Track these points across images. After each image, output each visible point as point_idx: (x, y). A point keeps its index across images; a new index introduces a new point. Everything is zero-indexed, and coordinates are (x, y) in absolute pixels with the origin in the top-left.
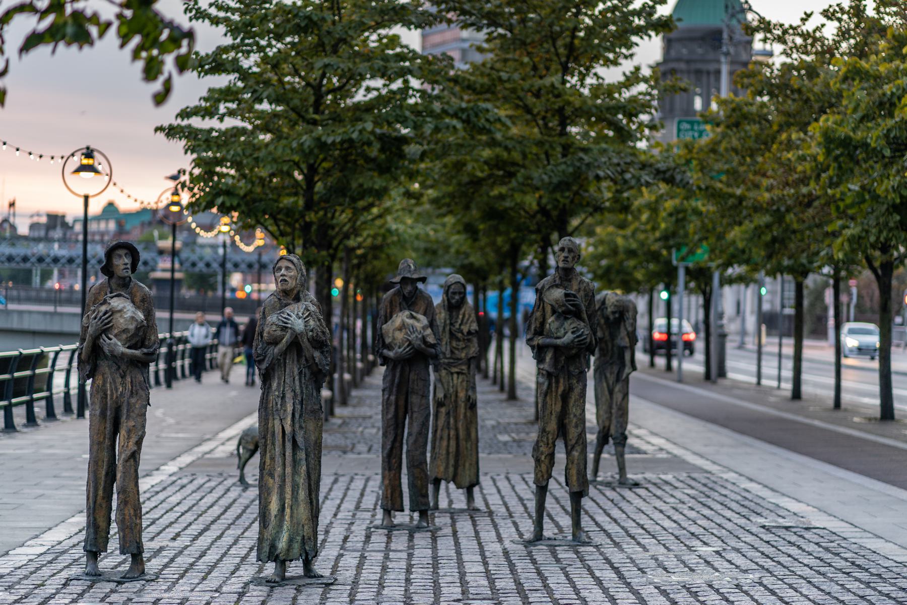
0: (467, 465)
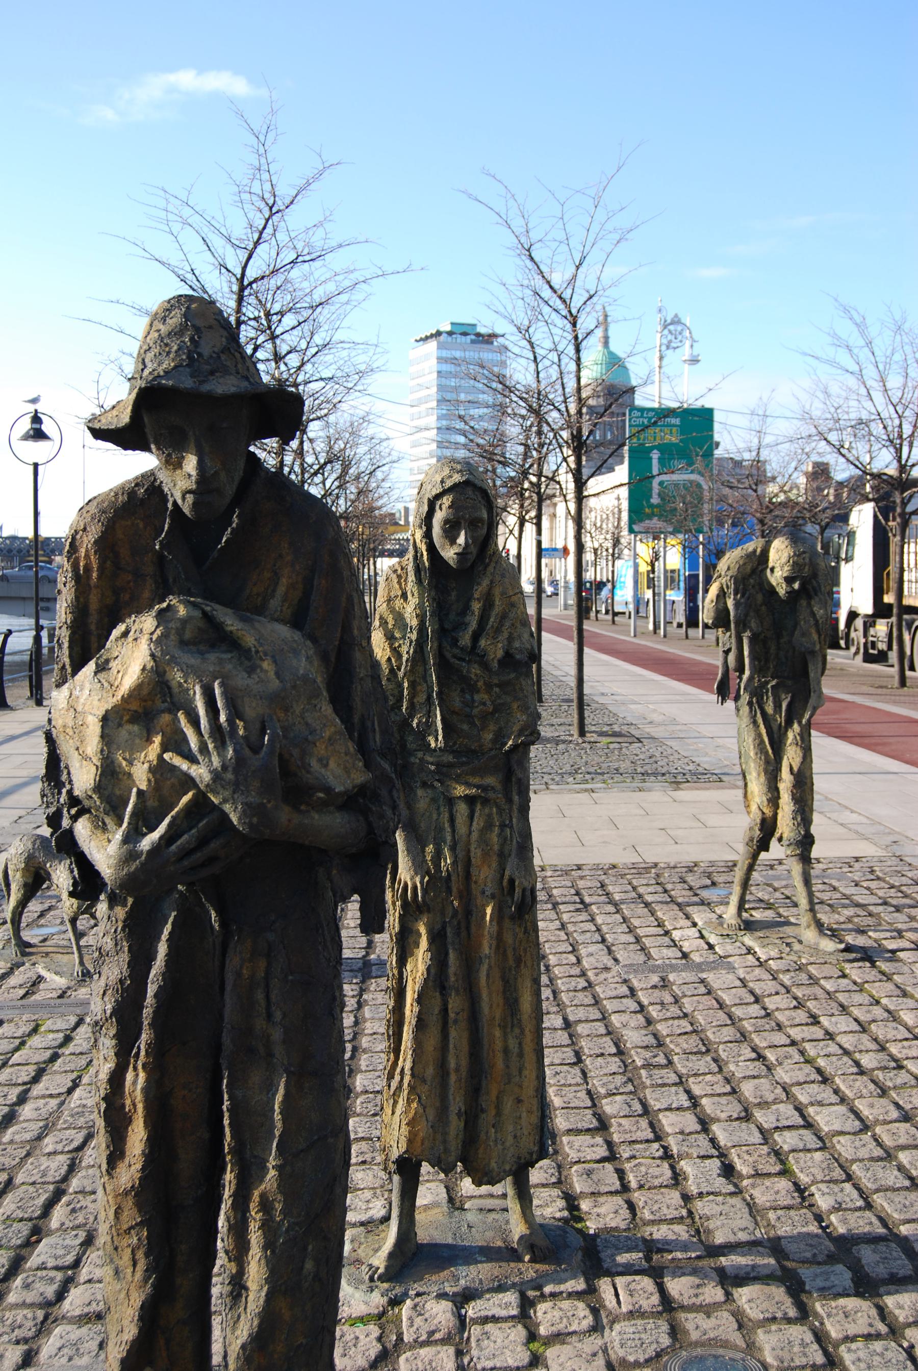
0: (508, 1104)
